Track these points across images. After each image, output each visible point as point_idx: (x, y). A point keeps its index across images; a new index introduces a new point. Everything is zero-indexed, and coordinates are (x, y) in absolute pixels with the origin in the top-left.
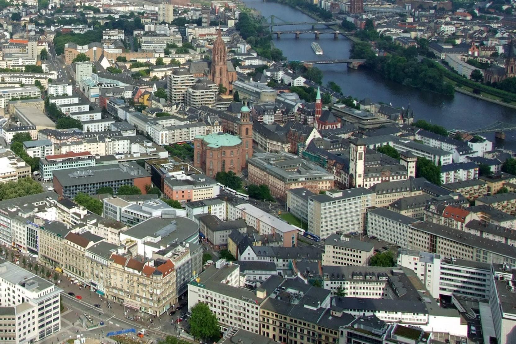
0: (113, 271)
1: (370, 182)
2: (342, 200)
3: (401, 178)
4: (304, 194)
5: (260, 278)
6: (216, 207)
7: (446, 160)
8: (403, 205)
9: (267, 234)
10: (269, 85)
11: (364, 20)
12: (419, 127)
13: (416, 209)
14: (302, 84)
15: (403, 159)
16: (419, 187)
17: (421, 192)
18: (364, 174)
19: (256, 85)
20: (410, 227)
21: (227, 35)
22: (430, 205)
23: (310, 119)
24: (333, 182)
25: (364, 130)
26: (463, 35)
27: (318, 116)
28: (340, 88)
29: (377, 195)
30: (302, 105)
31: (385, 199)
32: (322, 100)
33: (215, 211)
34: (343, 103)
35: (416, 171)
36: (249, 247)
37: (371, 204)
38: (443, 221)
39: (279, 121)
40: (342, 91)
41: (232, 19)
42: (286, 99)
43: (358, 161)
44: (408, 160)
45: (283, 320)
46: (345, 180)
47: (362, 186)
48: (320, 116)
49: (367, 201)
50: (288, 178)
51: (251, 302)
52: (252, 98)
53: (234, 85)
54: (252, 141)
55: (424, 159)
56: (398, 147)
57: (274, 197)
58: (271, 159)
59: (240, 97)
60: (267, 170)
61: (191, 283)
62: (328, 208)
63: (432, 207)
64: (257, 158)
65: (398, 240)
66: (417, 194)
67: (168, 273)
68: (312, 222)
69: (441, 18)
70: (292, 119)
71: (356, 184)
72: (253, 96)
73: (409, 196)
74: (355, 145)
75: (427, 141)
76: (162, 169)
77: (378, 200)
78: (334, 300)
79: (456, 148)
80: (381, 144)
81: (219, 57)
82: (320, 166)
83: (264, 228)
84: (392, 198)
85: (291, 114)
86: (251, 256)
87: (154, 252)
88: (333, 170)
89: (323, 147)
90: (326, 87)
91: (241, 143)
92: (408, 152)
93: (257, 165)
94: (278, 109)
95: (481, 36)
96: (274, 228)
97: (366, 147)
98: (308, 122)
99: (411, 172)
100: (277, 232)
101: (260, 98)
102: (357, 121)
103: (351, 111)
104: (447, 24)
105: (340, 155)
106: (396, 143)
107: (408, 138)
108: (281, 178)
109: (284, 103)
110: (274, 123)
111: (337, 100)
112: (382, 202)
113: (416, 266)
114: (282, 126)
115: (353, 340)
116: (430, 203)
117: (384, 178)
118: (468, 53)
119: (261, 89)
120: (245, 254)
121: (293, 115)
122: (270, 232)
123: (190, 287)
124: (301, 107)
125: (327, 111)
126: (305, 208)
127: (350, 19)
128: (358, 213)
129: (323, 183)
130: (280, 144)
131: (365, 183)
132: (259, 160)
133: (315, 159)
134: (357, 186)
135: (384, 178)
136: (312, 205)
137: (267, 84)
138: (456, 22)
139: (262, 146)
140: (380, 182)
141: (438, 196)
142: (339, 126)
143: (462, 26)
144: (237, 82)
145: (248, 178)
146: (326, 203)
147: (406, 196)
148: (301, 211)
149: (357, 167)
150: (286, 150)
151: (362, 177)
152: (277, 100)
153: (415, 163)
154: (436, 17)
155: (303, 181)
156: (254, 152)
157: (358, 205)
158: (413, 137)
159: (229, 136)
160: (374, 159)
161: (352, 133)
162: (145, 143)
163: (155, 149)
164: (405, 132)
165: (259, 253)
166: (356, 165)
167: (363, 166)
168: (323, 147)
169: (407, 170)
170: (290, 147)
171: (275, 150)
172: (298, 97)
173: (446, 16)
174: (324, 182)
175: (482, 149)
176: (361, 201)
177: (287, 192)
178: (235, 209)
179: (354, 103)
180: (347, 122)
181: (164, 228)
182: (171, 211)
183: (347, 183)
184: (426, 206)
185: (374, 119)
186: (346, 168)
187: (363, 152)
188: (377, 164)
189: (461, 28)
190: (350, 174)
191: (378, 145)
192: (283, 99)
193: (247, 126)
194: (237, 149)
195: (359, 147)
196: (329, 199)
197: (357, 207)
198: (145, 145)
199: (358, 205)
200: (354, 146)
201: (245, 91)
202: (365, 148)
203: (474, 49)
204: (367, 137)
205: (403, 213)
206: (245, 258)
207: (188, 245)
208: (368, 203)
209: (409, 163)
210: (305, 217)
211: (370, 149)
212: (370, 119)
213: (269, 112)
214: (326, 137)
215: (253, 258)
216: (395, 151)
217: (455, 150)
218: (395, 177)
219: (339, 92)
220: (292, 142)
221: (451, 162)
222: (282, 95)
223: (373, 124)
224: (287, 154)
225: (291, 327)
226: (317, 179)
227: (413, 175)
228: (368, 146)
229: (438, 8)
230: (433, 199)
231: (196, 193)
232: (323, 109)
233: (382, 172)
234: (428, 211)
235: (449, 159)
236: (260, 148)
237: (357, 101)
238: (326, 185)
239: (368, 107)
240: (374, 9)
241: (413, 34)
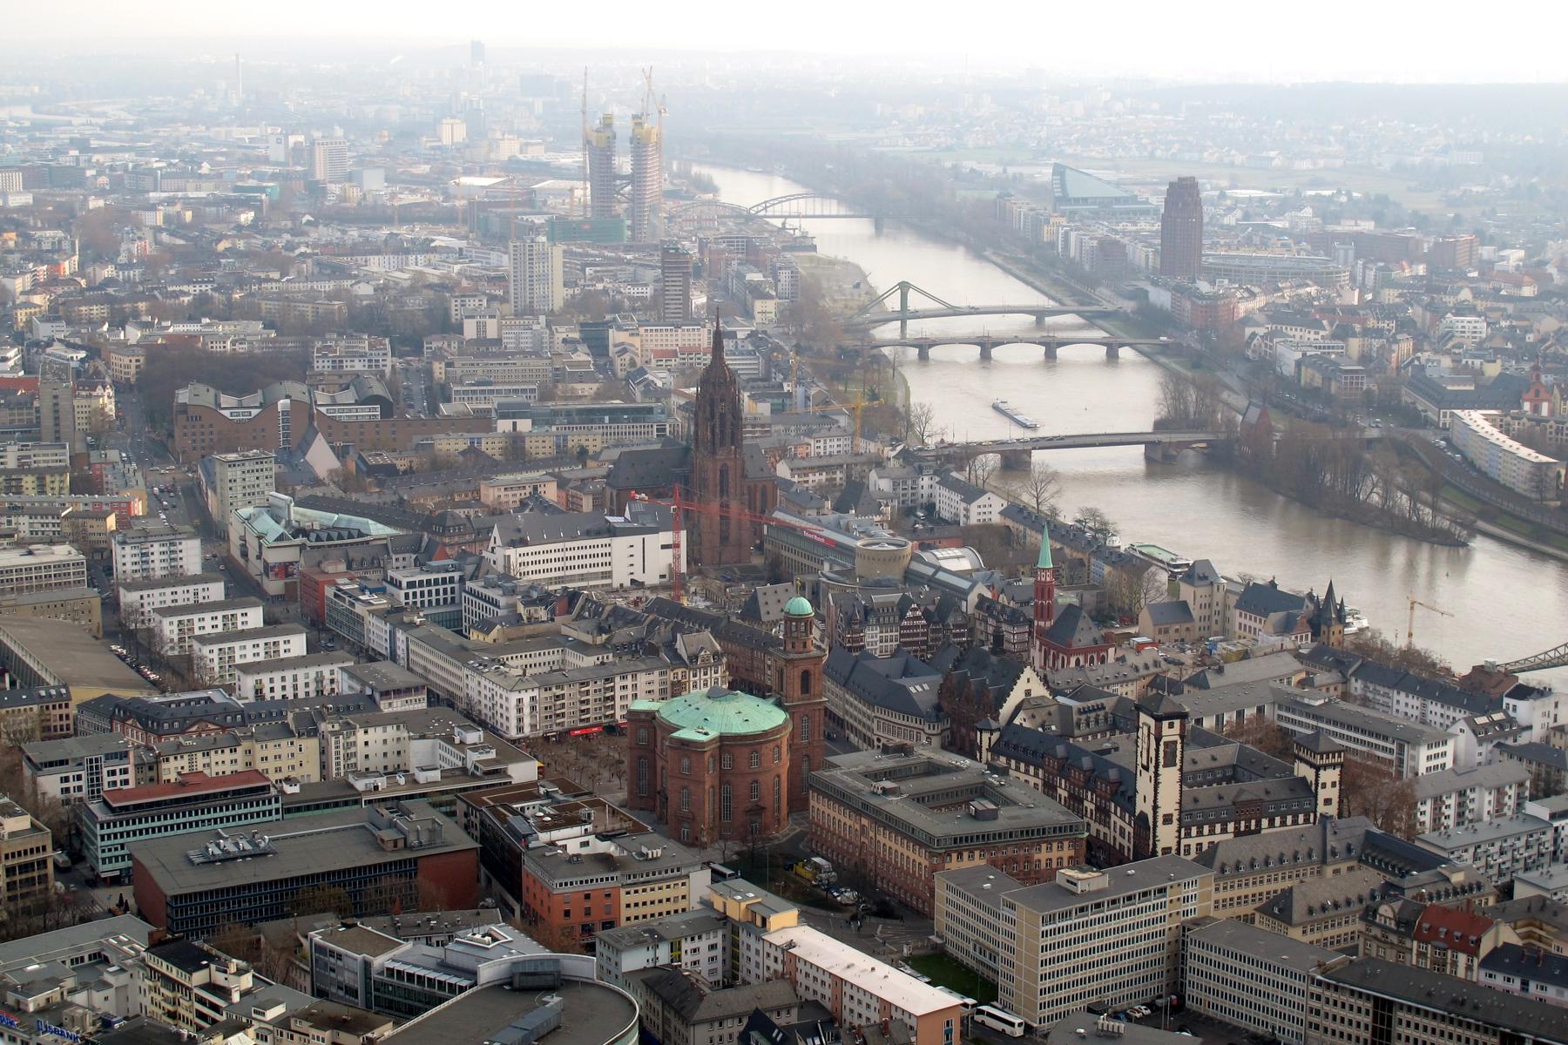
1: (1199, 840)
6: (696, 944)
7: (1437, 756)
8: (1298, 912)
9: (863, 1022)
11: (1202, 297)
14: (996, 519)
15: (1302, 760)
18: (1181, 812)
20: (1313, 979)
21: (749, 353)
26: (1510, 346)
31: (1243, 892)
33: (695, 958)
38: (1415, 952)
41: (768, 297)
42: (939, 569)
43: (1161, 770)
44: (1318, 762)
47: (1173, 852)
49: (1186, 900)
54: (820, 717)
63: (1385, 910)
64: (837, 773)
65: (1278, 1022)
68: (1012, 979)
71: (1155, 845)
74: (1153, 717)
75: (1382, 699)
77: (1222, 895)
81: (718, 431)
83: (854, 1005)
84: (1264, 888)
88: (1086, 803)
95: (1561, 351)
96: (886, 1005)
98: (1006, 645)
99: (1328, 802)
104: (1461, 310)
106: (1288, 710)
118: (1520, 407)
122: (875, 1017)
124: (988, 595)
127: (1161, 297)
131: (1184, 842)
138: (1489, 304)
143: (1509, 317)
151: (1175, 823)
153: (1338, 770)
154: (1431, 289)
157: (1159, 913)
173: (1460, 284)
175: (1546, 720)
176: (1167, 899)
178: (759, 946)
182: (542, 961)
186: (1124, 793)
189: (1503, 324)
192: (929, 571)
195: (1165, 724)
197: (1154, 921)
198: (457, 741)
199: (1159, 913)
200: (1152, 722)
202: (1183, 727)
203: (1537, 393)
208: (1190, 906)
209: (1322, 772)
210: (991, 963)
217: (1462, 725)
221: (1449, 765)
222: (926, 556)
227: (1332, 810)
228: (1199, 721)
231: (633, 898)
235: (1444, 754)
238: (1060, 854)
240: (1237, 262)
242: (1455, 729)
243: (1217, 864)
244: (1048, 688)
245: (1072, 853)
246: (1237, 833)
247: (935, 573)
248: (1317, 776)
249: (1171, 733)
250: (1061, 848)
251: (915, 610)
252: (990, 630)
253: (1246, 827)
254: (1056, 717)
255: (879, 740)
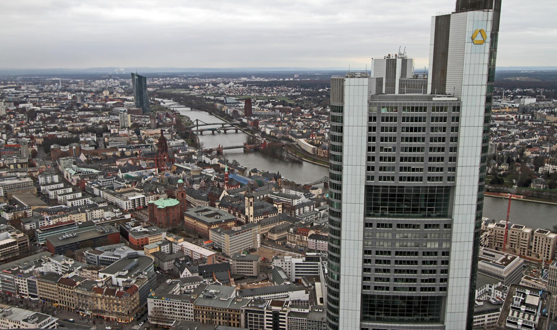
0: (95, 299)
5: (194, 286)
6: (164, 246)
11: (252, 120)
14: (217, 163)
23: (221, 184)
30: (216, 175)
36: (186, 269)
45: (208, 310)
51: (188, 302)
61: (149, 298)
67: (134, 293)
69: (296, 118)
76: (127, 226)
78: (238, 293)
79: (304, 194)
83: (195, 255)
86: (187, 274)
87: (123, 282)
96: (201, 255)
99: (280, 211)
100: (203, 256)
104: (299, 121)
110: (199, 189)
113: (282, 265)
115: (248, 313)
120: (184, 273)
122: (199, 257)
123: (149, 300)
124: (216, 177)
127: (245, 120)
139: (193, 204)
141: (294, 223)
154: (293, 117)
157: (251, 233)
159: (171, 200)
162: (114, 210)
163: (121, 213)
165: (192, 272)
181: (130, 265)
182: (134, 253)
186: (243, 212)
192: (205, 173)
199: (251, 233)
202: (253, 199)
206: (184, 276)
207: (146, 273)
215: (189, 275)
217: (303, 195)
222: (204, 170)
225: (213, 313)
227: (281, 212)
229: (294, 111)
230: (292, 225)
236: (192, 205)
241: (280, 128)
242: (301, 196)
246: (264, 218)
249: (251, 200)
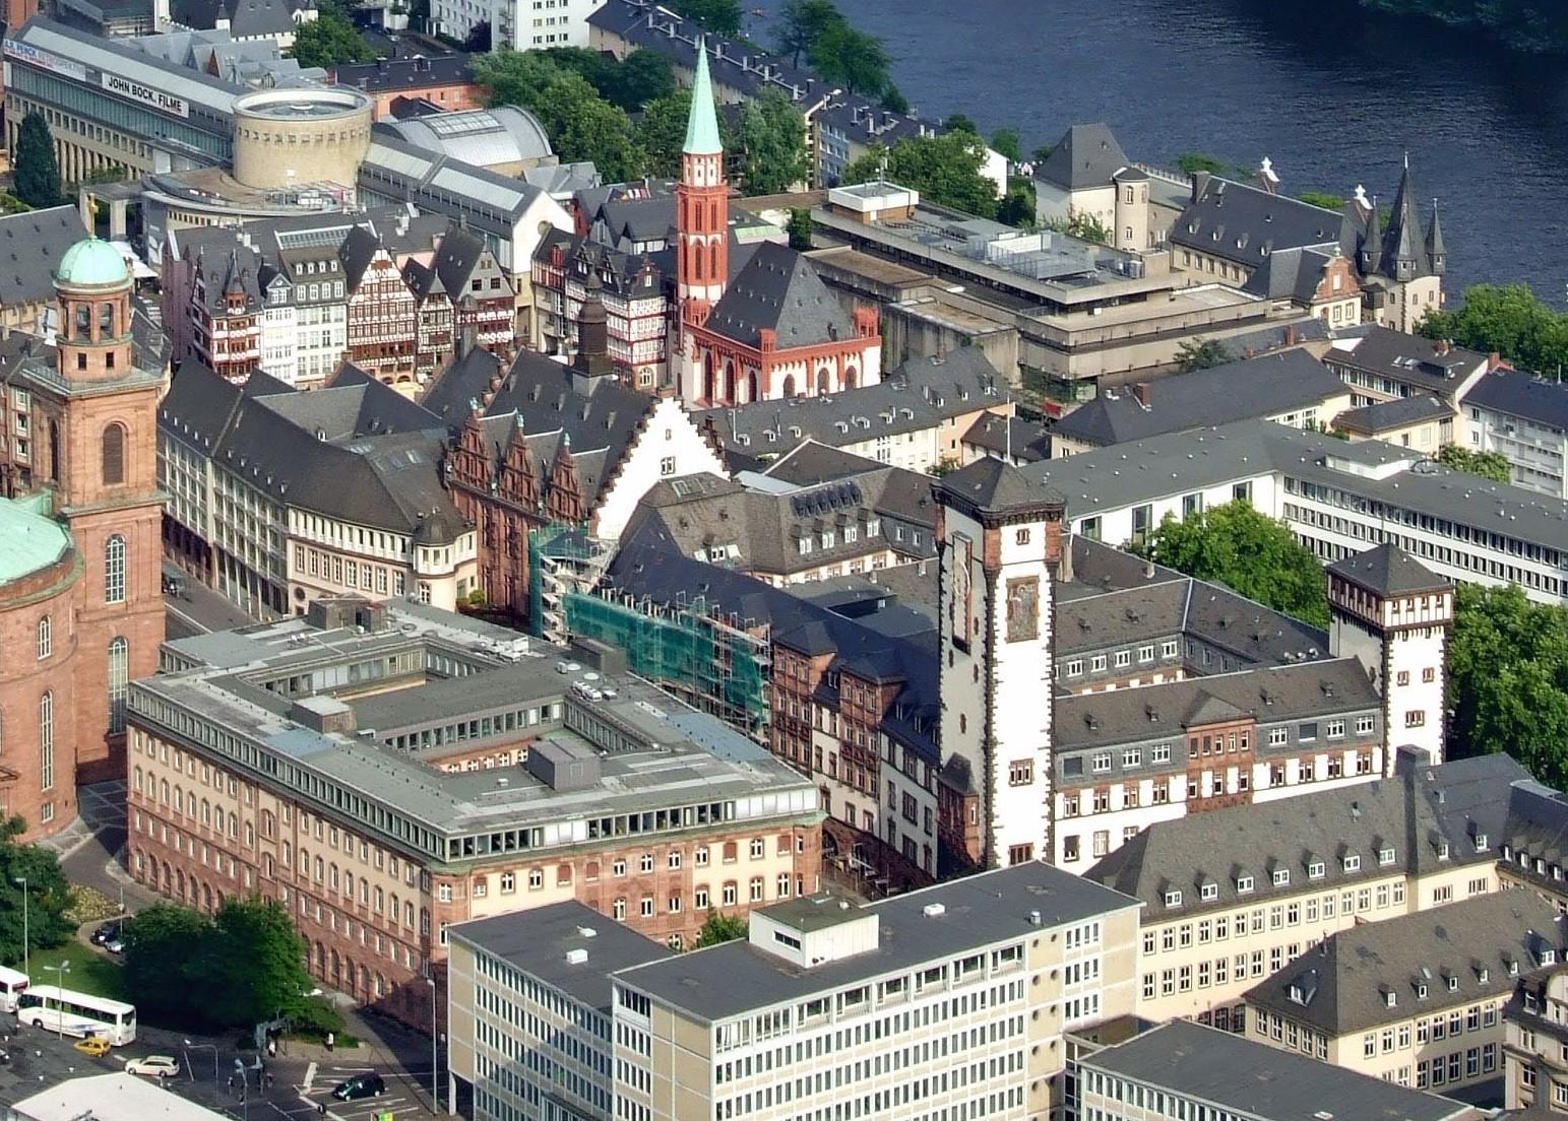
1: (1103, 821)
2: (873, 982)
3: (1334, 771)
4: (578, 956)
8: (1350, 988)
10: (306, 53)
12: (1478, 343)
13: (1447, 1016)
14: (580, 36)
15: (1348, 616)
16: (1472, 834)
17: (1487, 871)
18: (1054, 752)
19: (201, 54)
22: (1549, 974)
24: (814, 838)
25: (1063, 387)
27: (697, 291)
28: (885, 50)
29: (1145, 921)
30: (575, 205)
31: (1213, 951)
32: (732, 162)
34: (902, 174)
35: (1447, 704)
37: (1112, 998)
39: (387, 350)
40: (896, 77)
43: (1001, 649)
46: (910, 815)
47: (1038, 854)
48: (715, 293)
49: (1072, 975)
50: (453, 831)
52: (162, 166)
53: (17, 64)
54: (151, 537)
55: (1499, 607)
56: (1323, 521)
57: (343, 1000)
58: (318, 679)
59: (70, 166)
60: (283, 774)
62: (765, 1061)
64: (197, 681)
66: (1461, 894)
70: (486, 327)
71: (989, 839)
72: (177, 154)
73: (1398, 910)
74: (976, 516)
75: (1539, 463)
77: (1160, 962)
80: (1189, 502)
82: (713, 709)
85: (487, 292)
88: (817, 738)
89: (733, 551)
90: (768, 44)
91: (67, 555)
92: (1387, 550)
93: (199, 733)
94: (381, 255)
97: (1076, 528)
98: (613, 350)
99: (1414, 718)
101: (229, 167)
102: (1007, 317)
103: (961, 236)
105: (866, 607)
106: (1307, 489)
107: (1395, 437)
108: (398, 832)
109: (432, 200)
110: (345, 374)
111: (856, 154)
112: (1195, 975)
114: (408, 390)
116: (1549, 960)
117: (1207, 779)
119: (240, 91)
121: (504, 291)
124: (566, 223)
125: (767, 246)
126: (591, 1076)
128: (1004, 1083)
129: (730, 851)
130: (390, 547)
131: (1063, 830)
132: (215, 692)
133: (668, 654)
134: (1004, 861)
135: (1207, 779)
136: (643, 1042)
137: (287, 39)
139: (245, 574)
140: (1176, 811)
142: (869, 366)
144: (38, 35)
145: (125, 862)
146: (752, 1015)
147: (1375, 914)
148: (555, 1099)
149: (998, 700)
150: (443, 596)
151: (1041, 782)
152: (371, 180)
153: (1438, 636)
155: (575, 847)
156: (175, 629)
157: (1006, 1011)
158: (1434, 427)
160: (1133, 627)
161: (973, 417)
164: (1380, 394)
166: (989, 686)
167: (1045, 692)
168: (733, 551)
169: (1382, 701)
170: (471, 571)
171: (342, 602)
172: (540, 144)
174: (743, 846)
177: (443, 949)
179: (984, 172)
180: (929, 336)
183: (922, 838)
184: (1520, 990)
185: (1140, 297)
187: (1045, 575)
188: (1152, 668)
190: (944, 762)
191: (1167, 508)
193: (107, 412)
194: (29, 615)
195: (1008, 532)
196: (781, 980)
199: (1006, 1011)
201: (107, 113)
202: (1055, 541)
204: (1084, 449)
205: (1349, 1052)
208: (1079, 991)
209: (1397, 645)
211: (1105, 549)
212: (1105, 303)
213: (305, 279)
214: (758, 465)
216: (1298, 556)
218: (1293, 768)
219: (873, 86)
220: (489, 527)
222: (412, 130)
223: (1131, 340)
224: (444, 632)
226: (689, 819)
227: (1430, 739)
232: (746, 236)
233: (1194, 732)
234: (1535, 1025)
236: (234, 593)
237: (1012, 157)
238: (757, 868)
239: (1092, 202)
243: (1147, 882)
244: (719, 452)
245: (787, 864)
247: (432, 173)
248: (1385, 654)
250: (757, 851)
251: (383, 265)
252: (573, 310)
253: (1217, 786)
254: (738, 522)
255: (300, 595)
